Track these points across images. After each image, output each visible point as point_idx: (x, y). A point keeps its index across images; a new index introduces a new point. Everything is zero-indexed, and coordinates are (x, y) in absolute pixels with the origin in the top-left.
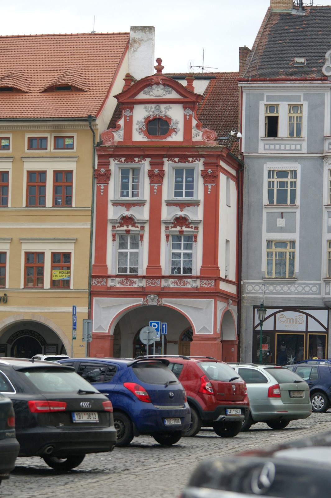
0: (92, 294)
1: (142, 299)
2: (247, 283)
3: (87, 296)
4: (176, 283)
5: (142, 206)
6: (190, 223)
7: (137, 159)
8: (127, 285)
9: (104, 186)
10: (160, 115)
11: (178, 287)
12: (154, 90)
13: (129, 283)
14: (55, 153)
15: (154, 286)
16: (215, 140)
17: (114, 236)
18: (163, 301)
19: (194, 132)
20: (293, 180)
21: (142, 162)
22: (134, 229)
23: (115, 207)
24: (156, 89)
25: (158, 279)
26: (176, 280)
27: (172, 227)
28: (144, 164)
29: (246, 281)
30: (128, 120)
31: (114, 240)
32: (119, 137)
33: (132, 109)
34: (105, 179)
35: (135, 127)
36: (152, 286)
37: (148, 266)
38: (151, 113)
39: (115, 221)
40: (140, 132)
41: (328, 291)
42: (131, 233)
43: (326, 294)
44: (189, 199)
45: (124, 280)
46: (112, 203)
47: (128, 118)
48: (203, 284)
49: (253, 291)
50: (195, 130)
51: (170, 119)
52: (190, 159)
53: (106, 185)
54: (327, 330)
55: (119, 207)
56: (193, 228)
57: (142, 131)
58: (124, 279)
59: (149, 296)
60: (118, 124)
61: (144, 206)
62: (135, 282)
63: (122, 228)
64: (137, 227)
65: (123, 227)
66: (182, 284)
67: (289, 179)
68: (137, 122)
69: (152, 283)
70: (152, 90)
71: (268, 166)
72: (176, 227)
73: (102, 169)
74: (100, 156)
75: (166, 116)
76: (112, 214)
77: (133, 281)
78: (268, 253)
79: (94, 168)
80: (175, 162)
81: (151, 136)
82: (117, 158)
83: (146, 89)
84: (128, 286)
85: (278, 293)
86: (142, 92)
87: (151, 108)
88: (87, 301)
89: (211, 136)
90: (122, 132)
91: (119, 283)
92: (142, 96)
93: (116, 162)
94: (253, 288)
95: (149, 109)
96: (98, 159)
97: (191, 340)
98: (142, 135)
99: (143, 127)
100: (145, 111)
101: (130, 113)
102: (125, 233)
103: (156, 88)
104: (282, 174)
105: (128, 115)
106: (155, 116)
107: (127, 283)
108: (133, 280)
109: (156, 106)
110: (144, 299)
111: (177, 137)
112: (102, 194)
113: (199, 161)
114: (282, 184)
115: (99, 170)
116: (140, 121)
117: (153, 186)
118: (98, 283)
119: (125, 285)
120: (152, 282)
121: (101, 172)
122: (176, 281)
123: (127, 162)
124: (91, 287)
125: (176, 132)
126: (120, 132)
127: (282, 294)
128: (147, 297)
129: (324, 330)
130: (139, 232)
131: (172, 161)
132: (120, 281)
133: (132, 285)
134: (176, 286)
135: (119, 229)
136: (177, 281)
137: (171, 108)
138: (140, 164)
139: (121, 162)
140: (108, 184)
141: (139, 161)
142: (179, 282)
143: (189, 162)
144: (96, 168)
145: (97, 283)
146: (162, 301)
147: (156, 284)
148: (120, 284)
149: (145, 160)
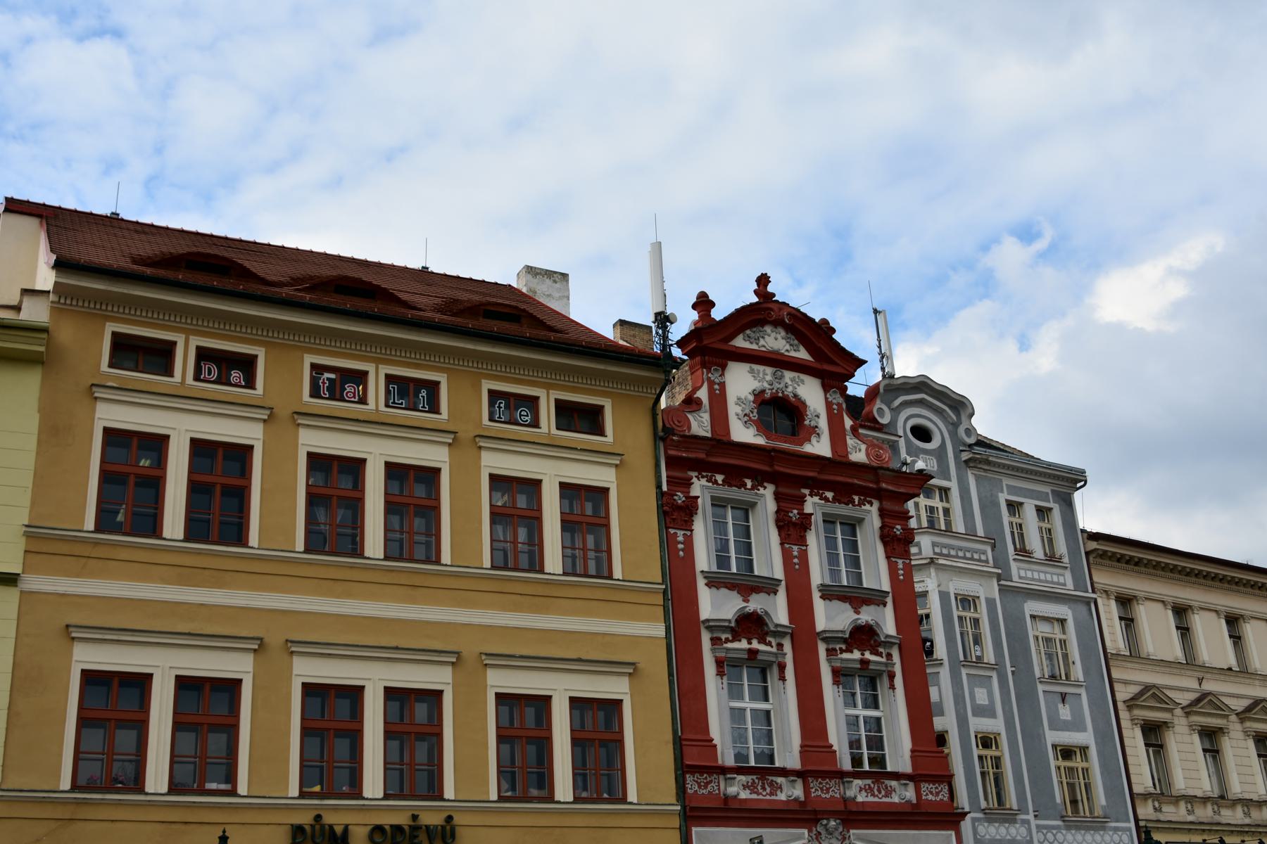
1: (806, 831)
3: (676, 822)
4: (869, 790)
5: (772, 595)
6: (880, 644)
8: (764, 793)
9: (684, 534)
10: (785, 393)
11: (876, 799)
12: (769, 336)
13: (768, 790)
14: (561, 438)
15: (828, 796)
17: (719, 663)
18: (852, 837)
19: (851, 441)
21: (759, 490)
22: (762, 647)
23: (714, 590)
24: (773, 335)
25: (833, 778)
26: (869, 782)
27: (842, 651)
28: (763, 496)
30: (717, 392)
31: (720, 673)
32: (699, 426)
33: (724, 367)
34: (686, 519)
35: (733, 410)
36: (824, 796)
37: (801, 747)
38: (766, 385)
39: (727, 624)
40: (746, 422)
42: (760, 657)
45: (756, 781)
46: (706, 581)
47: (716, 387)
48: (927, 794)
50: (851, 439)
51: (804, 404)
53: (689, 533)
55: (724, 591)
56: (884, 655)
58: (757, 778)
59: (825, 822)
60: (695, 396)
61: (776, 595)
62: (781, 785)
63: (736, 645)
64: (770, 644)
65: (740, 641)
66: (883, 793)
68: (736, 399)
69: (822, 789)
70: (765, 335)
72: (852, 652)
73: (677, 493)
74: (671, 463)
75: (796, 396)
76: (709, 608)
77: (777, 784)
79: (659, 486)
80: (826, 499)
82: (704, 474)
83: (748, 332)
84: (768, 797)
86: (741, 336)
87: (765, 374)
89: (884, 457)
90: (706, 417)
91: (744, 789)
92: (740, 342)
93: (704, 482)
95: (761, 375)
96: (667, 470)
99: (752, 413)
100: (753, 378)
101: (720, 376)
102: (746, 656)
103: (772, 332)
105: (717, 381)
106: (774, 391)
107: (764, 789)
108: (775, 782)
109: (776, 371)
110: (810, 831)
111: (821, 447)
112: (681, 553)
113: (871, 506)
115: (670, 494)
116: (743, 397)
117: (790, 551)
118: (700, 787)
119: (761, 794)
120: (821, 786)
121: (675, 500)
122: (869, 785)
123: (728, 486)
125: (818, 434)
126: (702, 415)
128: (816, 827)
130: (777, 657)
131: (818, 497)
132: (748, 782)
133: (776, 795)
134: (871, 799)
135: (729, 645)
136: (872, 786)
137: (803, 382)
138: (757, 493)
140: (692, 531)
142: (876, 788)
144: (665, 488)
145: (697, 788)
146: (850, 836)
147: (831, 793)
148: (748, 791)
149: (765, 488)
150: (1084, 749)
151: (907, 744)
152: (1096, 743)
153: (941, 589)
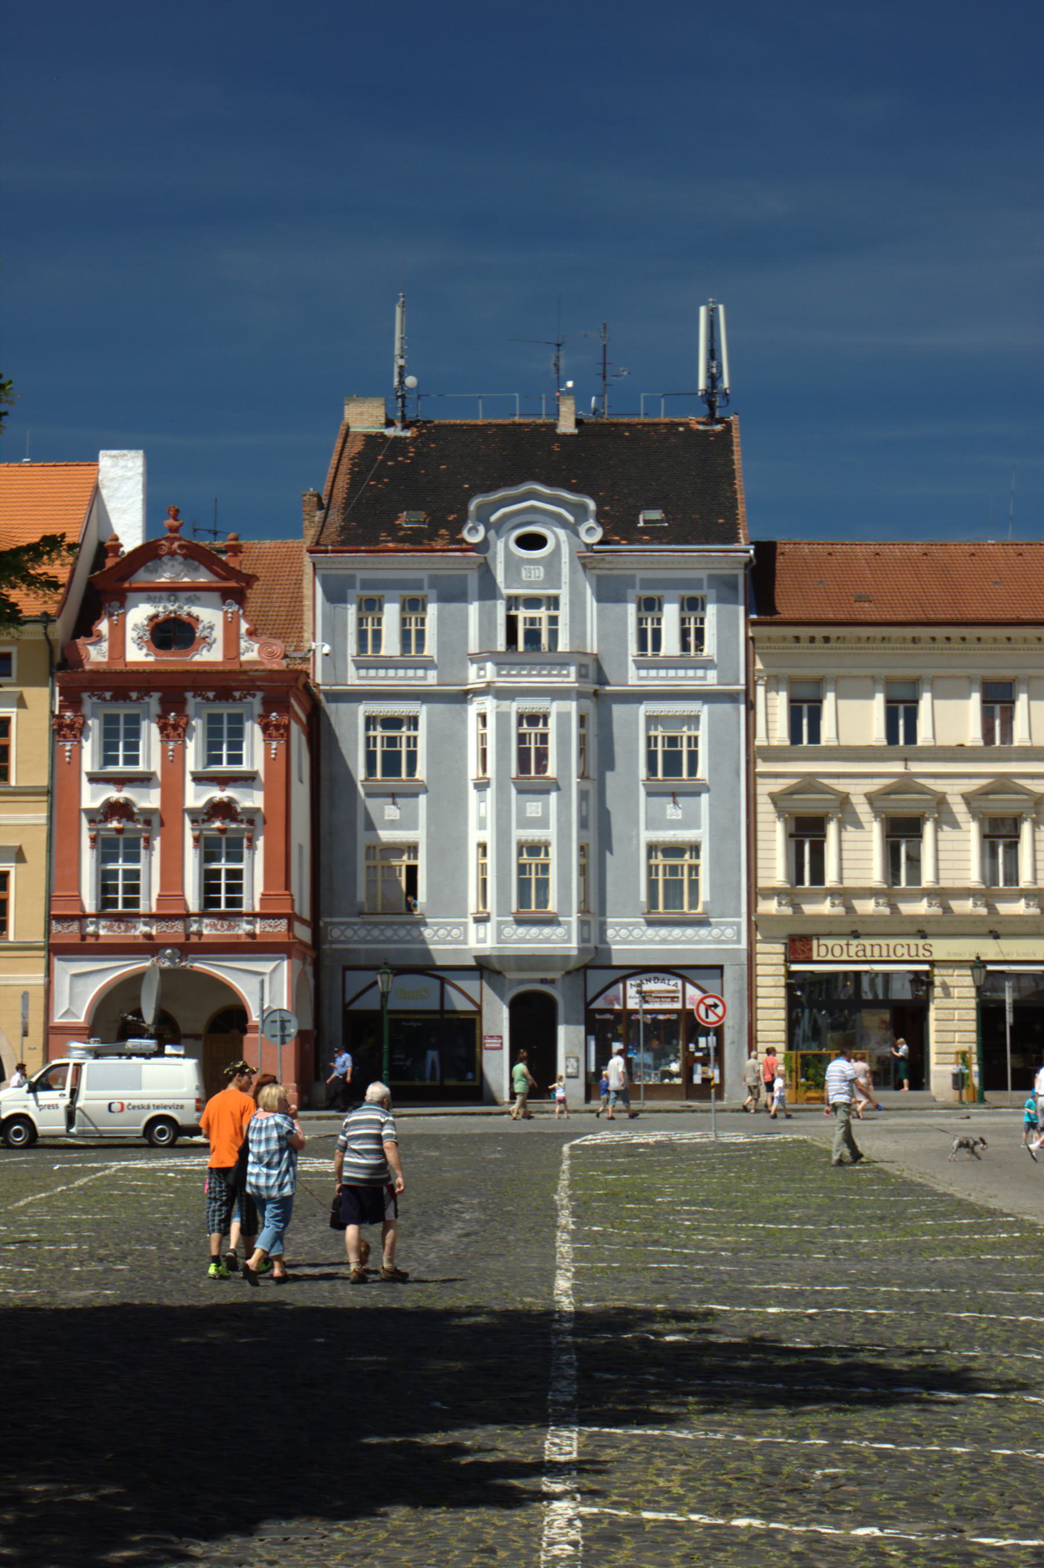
0: (55, 950)
2: (332, 923)
4: (214, 926)
7: (134, 695)
11: (219, 933)
16: (283, 658)
19: (243, 644)
20: (412, 733)
23: (94, 785)
24: (170, 563)
29: (328, 920)
35: (130, 634)
41: (481, 936)
43: (479, 941)
44: (235, 768)
49: (342, 938)
51: (197, 619)
52: (237, 694)
54: (480, 1007)
57: (143, 641)
67: (405, 732)
71: (363, 709)
78: (368, 867)
79: (52, 712)
80: (208, 699)
81: (162, 652)
83: (149, 564)
85: (389, 941)
86: (143, 569)
88: (43, 962)
90: (105, 645)
92: (142, 577)
93: (95, 699)
94: (343, 932)
97: (245, 1031)
98: (145, 651)
104: (392, 723)
111: (211, 655)
114: (392, 741)
124: (49, 938)
127: (396, 942)
129: (473, 1008)
134: (214, 932)
139: (105, 700)
141: (138, 699)
143: (234, 699)
144: (57, 712)
149: (151, 696)
150: (695, 849)
151: (259, 888)
152: (711, 840)
153: (499, 710)
